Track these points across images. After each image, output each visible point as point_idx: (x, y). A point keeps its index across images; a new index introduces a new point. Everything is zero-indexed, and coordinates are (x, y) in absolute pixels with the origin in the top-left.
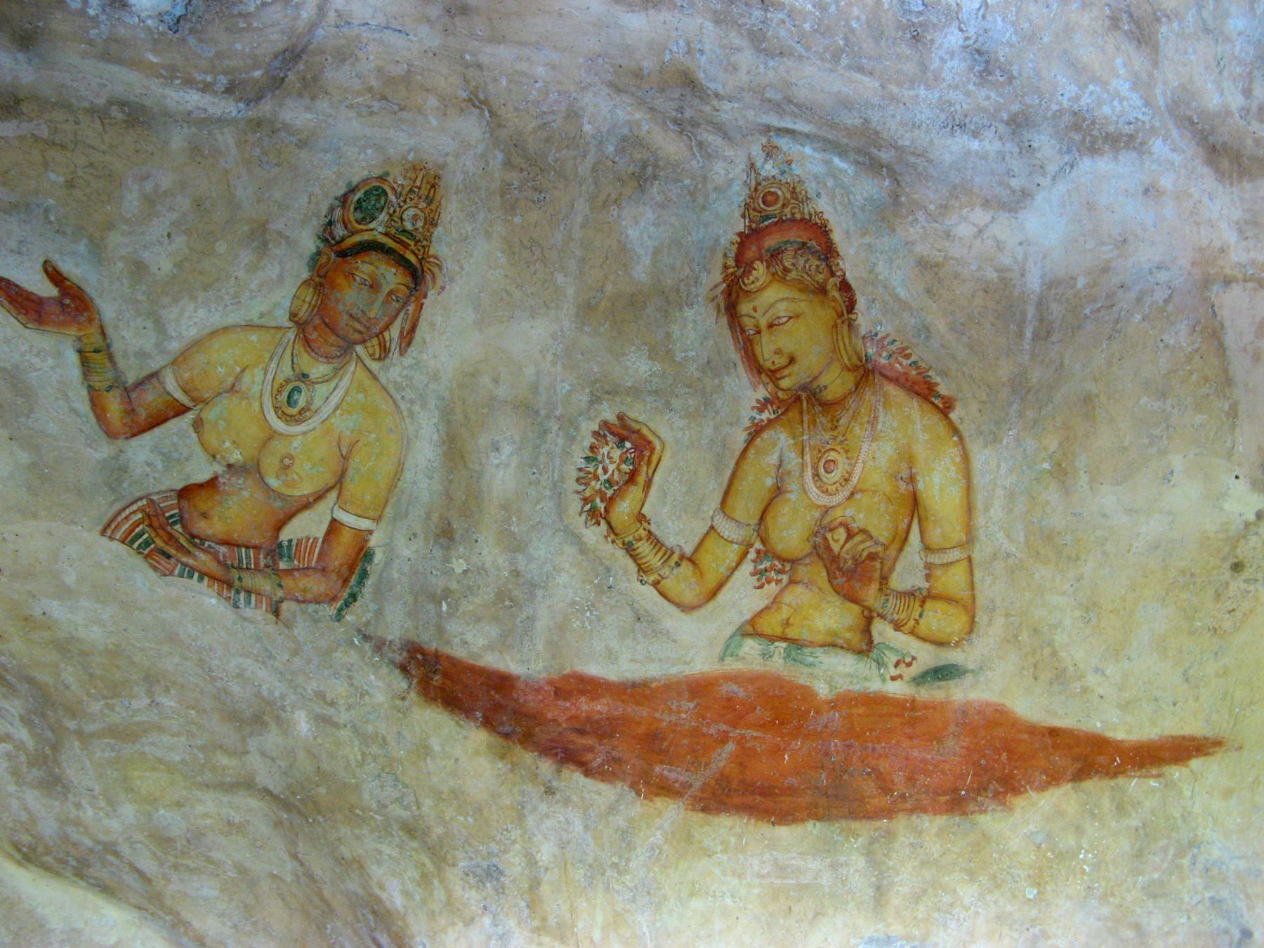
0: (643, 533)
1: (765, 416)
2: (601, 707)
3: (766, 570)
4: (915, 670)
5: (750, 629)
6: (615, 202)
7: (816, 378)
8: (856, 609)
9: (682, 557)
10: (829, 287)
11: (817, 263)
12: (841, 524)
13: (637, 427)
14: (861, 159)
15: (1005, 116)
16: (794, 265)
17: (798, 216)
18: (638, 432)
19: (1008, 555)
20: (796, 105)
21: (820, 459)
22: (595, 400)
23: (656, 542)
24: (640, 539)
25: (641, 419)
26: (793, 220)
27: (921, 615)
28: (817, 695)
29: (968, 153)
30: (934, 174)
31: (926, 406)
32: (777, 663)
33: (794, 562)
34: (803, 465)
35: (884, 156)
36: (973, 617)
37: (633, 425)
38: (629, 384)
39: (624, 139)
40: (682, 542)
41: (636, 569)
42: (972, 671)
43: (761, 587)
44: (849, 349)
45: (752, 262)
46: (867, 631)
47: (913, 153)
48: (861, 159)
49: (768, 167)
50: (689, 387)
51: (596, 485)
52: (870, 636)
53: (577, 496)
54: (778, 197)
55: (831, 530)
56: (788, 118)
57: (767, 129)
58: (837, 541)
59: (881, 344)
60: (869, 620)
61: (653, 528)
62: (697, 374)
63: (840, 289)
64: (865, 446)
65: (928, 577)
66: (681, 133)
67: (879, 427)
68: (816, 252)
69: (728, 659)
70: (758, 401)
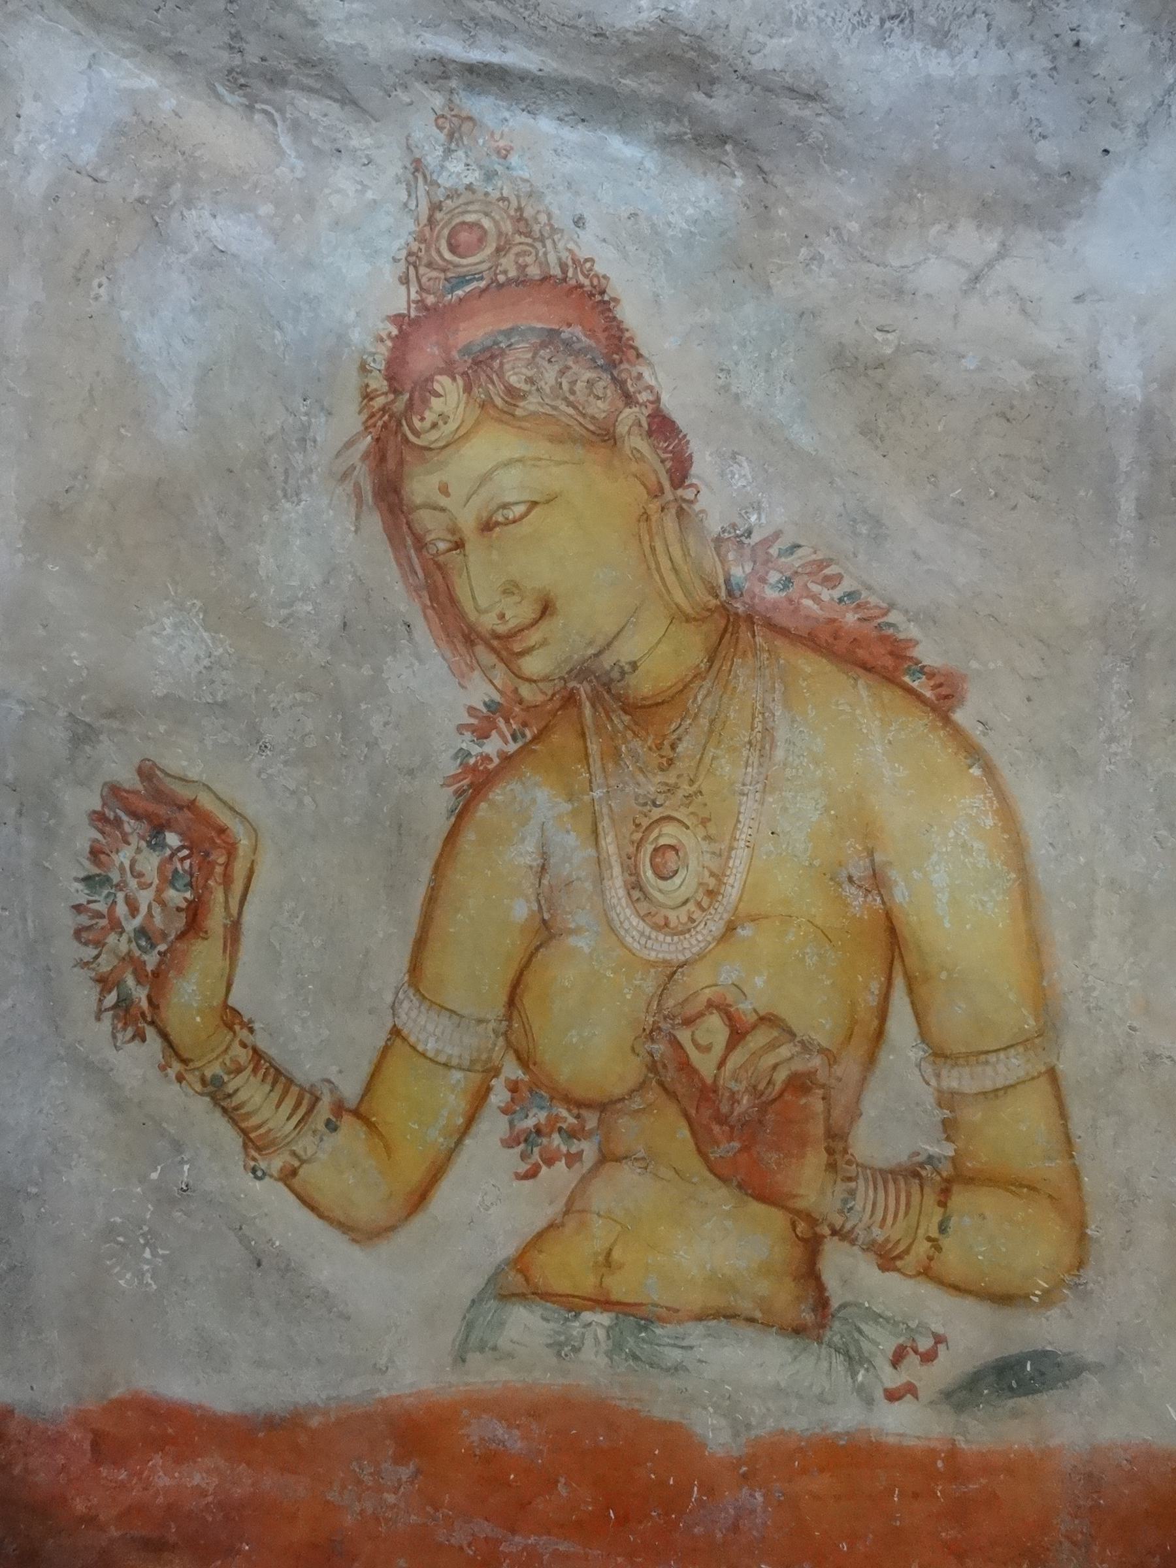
0: (243, 1055)
1: (493, 746)
2: (199, 1478)
3: (538, 1131)
5: (514, 1280)
7: (609, 645)
8: (777, 1219)
9: (339, 1108)
10: (622, 429)
11: (589, 375)
12: (711, 1005)
13: (185, 793)
14: (673, 129)
16: (530, 381)
17: (534, 272)
18: (191, 805)
19: (1154, 1058)
21: (639, 845)
22: (82, 736)
23: (277, 1077)
24: (239, 1070)
25: (192, 774)
26: (522, 281)
27: (943, 1229)
29: (928, 84)
31: (888, 694)
32: (593, 1363)
33: (603, 1107)
35: (722, 106)
36: (1082, 1225)
38: (159, 691)
39: (120, 130)
40: (332, 1072)
42: (1098, 1368)
43: (532, 1174)
44: (684, 568)
45: (430, 379)
46: (809, 1274)
47: (792, 91)
48: (673, 129)
49: (455, 166)
51: (121, 944)
52: (820, 1287)
54: (485, 232)
55: (688, 1022)
56: (485, 36)
57: (439, 71)
59: (761, 555)
60: (812, 1247)
63: (650, 433)
64: (749, 806)
65: (949, 1128)
66: (250, 108)
67: (779, 754)
69: (474, 1358)
70: (471, 710)
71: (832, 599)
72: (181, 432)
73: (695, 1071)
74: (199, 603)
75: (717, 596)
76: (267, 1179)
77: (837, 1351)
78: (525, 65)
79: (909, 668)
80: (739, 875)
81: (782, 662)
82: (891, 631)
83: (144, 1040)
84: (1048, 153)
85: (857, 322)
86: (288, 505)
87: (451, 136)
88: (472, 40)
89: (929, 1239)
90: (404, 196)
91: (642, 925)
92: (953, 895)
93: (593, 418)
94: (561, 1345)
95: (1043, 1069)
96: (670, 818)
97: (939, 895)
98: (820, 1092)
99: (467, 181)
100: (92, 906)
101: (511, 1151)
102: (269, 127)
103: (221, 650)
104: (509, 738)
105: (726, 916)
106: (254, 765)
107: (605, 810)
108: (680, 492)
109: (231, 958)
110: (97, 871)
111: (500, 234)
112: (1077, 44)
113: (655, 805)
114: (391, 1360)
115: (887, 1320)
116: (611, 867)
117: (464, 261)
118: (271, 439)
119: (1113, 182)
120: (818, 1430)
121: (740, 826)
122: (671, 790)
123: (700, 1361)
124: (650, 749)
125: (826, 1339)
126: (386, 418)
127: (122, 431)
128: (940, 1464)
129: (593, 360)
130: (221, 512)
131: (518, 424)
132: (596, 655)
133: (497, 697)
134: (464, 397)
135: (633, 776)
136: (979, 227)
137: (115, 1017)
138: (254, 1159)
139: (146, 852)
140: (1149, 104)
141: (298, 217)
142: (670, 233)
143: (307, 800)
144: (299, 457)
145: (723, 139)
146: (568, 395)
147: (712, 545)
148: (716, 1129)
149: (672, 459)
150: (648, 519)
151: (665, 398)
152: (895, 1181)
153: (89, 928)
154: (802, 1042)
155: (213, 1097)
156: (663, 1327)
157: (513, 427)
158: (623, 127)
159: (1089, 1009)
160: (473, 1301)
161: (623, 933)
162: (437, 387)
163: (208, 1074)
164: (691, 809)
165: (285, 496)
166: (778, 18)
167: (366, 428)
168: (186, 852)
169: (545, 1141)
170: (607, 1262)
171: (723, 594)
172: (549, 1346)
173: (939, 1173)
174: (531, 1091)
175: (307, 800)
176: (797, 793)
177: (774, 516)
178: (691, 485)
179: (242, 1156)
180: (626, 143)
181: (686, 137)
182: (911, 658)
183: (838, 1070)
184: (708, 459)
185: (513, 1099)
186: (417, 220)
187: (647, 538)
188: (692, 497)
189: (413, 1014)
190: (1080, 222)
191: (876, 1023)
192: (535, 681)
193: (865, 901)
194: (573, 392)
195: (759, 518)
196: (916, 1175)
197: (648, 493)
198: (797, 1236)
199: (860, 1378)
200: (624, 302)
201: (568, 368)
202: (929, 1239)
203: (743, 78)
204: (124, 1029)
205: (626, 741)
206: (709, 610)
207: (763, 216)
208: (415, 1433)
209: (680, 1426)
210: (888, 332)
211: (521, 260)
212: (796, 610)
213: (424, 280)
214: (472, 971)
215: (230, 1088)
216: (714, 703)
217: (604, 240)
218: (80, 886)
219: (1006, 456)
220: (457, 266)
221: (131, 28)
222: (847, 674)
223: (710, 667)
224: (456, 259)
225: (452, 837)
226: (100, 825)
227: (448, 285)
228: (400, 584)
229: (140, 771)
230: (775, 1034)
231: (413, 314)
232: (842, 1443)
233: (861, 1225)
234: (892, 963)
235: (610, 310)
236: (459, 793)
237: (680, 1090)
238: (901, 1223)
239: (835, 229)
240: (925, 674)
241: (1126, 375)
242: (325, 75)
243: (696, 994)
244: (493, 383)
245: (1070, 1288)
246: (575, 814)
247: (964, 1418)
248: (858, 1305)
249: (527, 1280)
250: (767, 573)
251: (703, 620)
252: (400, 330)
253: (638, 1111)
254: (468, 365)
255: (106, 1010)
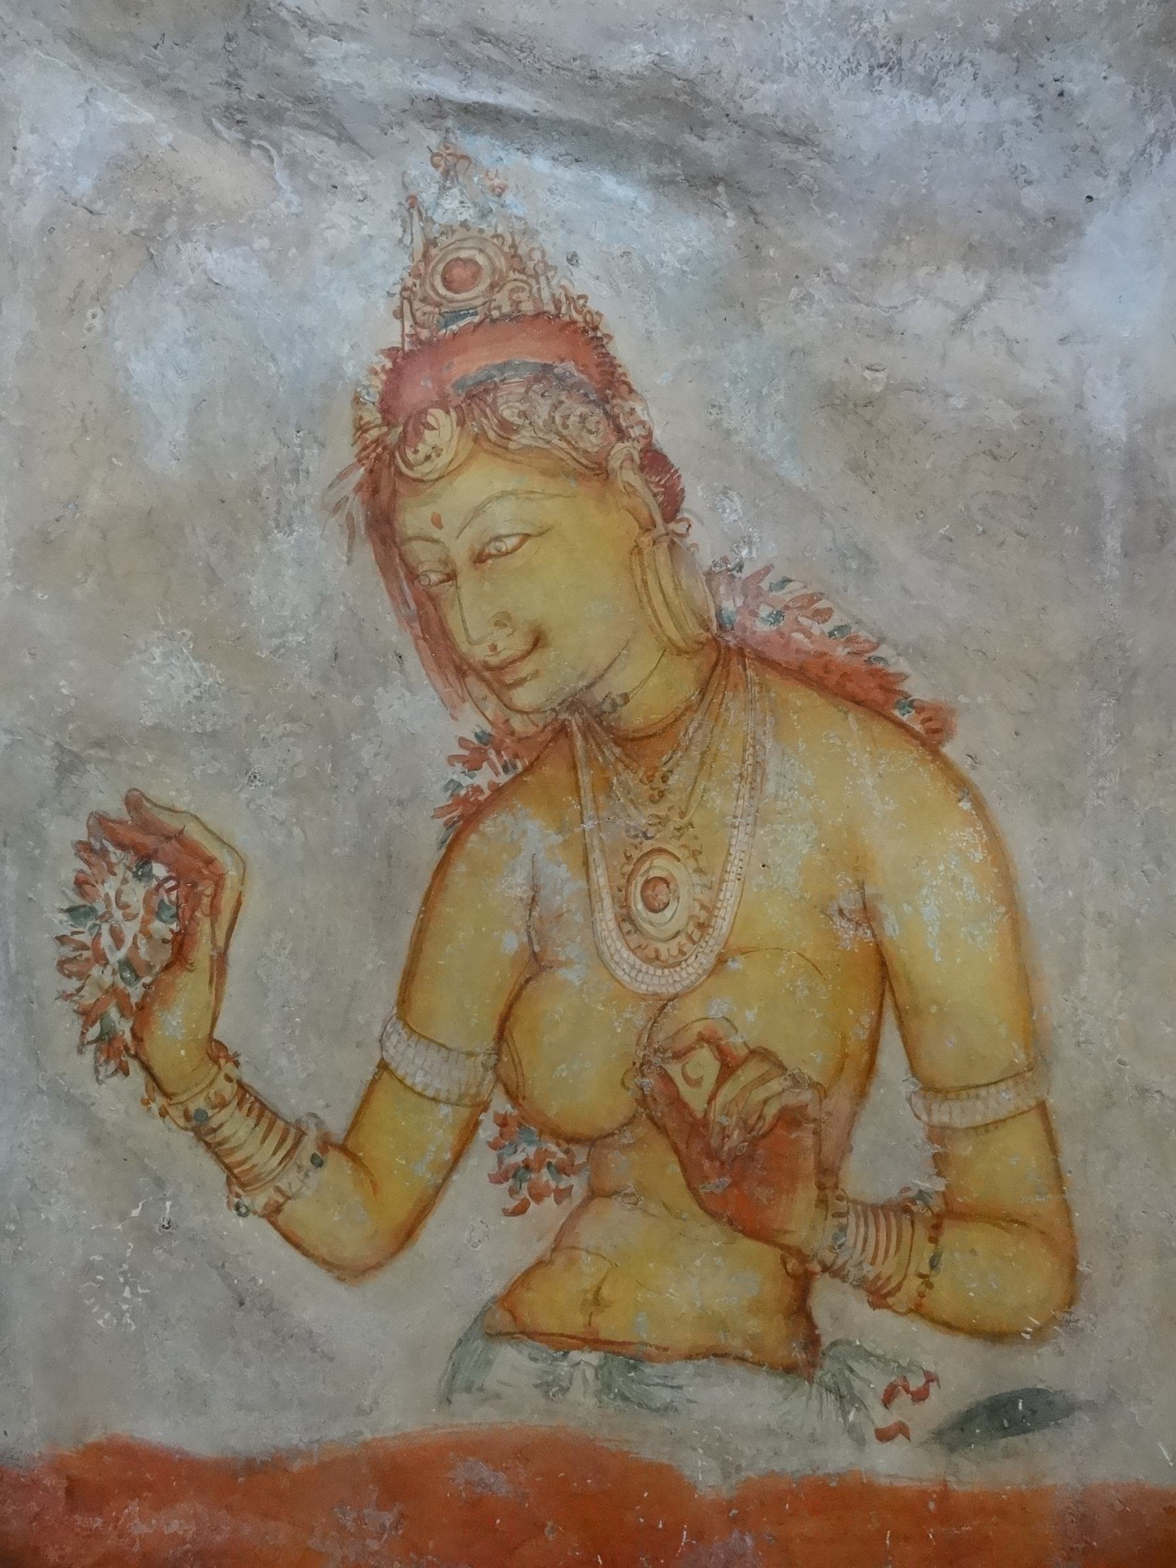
0: (228, 1090)
2: (177, 1524)
3: (527, 1167)
4: (939, 1407)
5: (501, 1319)
6: (96, 298)
7: (601, 677)
8: (768, 1255)
9: (325, 1143)
10: (614, 464)
11: (581, 409)
12: (702, 1039)
13: (173, 823)
14: (666, 170)
15: (994, 31)
16: (524, 415)
17: (528, 307)
18: (179, 836)
19: (1143, 1092)
20: (495, 40)
21: (630, 878)
22: (69, 765)
23: (262, 1111)
24: (224, 1105)
25: (180, 806)
26: (517, 317)
27: (933, 1264)
28: (693, 1488)
29: (915, 130)
30: (839, 185)
31: (879, 728)
33: (594, 1141)
34: (590, 895)
35: (715, 149)
36: (1073, 1262)
37: (165, 817)
41: (224, 1177)
43: (520, 1210)
44: (676, 602)
45: (425, 412)
46: (799, 1310)
47: (782, 135)
48: (666, 170)
49: (450, 203)
50: (292, 718)
52: (812, 1325)
53: (66, 1005)
55: (678, 1056)
56: (480, 77)
57: (435, 111)
58: (697, 1083)
59: (752, 590)
60: (802, 1284)
61: (247, 1074)
62: (310, 687)
63: (642, 468)
64: (740, 837)
65: (941, 1163)
66: (247, 143)
67: (770, 787)
68: (578, 385)
69: (461, 1398)
70: (462, 742)
71: (823, 633)
72: (174, 462)
73: (685, 1105)
74: (189, 633)
75: (708, 630)
76: (251, 1215)
77: (828, 1390)
78: (519, 105)
79: (898, 702)
80: (729, 909)
81: (773, 695)
82: (881, 665)
83: (127, 1073)
84: (1033, 198)
85: (847, 361)
86: (279, 536)
87: (446, 173)
88: (467, 81)
89: (921, 1276)
90: (399, 233)
91: (632, 957)
92: (943, 928)
93: (586, 451)
94: (548, 1384)
95: (1033, 1103)
96: (661, 851)
97: (930, 929)
98: (812, 1125)
99: (461, 218)
100: (76, 937)
101: (500, 1186)
102: (266, 163)
103: (211, 680)
104: (501, 770)
105: (717, 949)
106: (243, 796)
107: (596, 842)
108: (672, 526)
109: (217, 990)
110: (79, 901)
111: (494, 270)
112: (1061, 94)
113: (647, 838)
114: (376, 1402)
115: (878, 1358)
116: (602, 900)
117: (458, 297)
118: (264, 470)
119: (1096, 228)
120: (810, 1472)
121: (731, 858)
122: (662, 822)
123: (689, 1401)
124: (641, 781)
125: (816, 1379)
126: (379, 450)
127: (114, 460)
128: (932, 1506)
129: (586, 395)
130: (213, 542)
131: (510, 456)
132: (589, 687)
133: (488, 729)
134: (457, 430)
135: (623, 806)
136: (966, 269)
137: (98, 1050)
138: (238, 1196)
139: (133, 883)
140: (1131, 153)
141: (293, 251)
142: (663, 271)
143: (296, 830)
144: (292, 487)
145: (715, 181)
146: (560, 428)
147: (704, 578)
148: (707, 1165)
149: (664, 493)
150: (640, 553)
151: (657, 434)
152: (887, 1218)
153: (71, 960)
154: (793, 1076)
155: (196, 1131)
156: (653, 1367)
157: (505, 459)
158: (615, 169)
159: (1078, 1044)
160: (460, 1341)
161: (613, 966)
162: (430, 420)
163: (192, 1108)
164: (682, 841)
165: (277, 527)
166: (770, 65)
167: (359, 461)
168: (172, 883)
169: (533, 1176)
170: (597, 1301)
171: (714, 626)
172: (536, 1386)
173: (929, 1208)
174: (520, 1125)
175: (296, 830)
176: (788, 826)
177: (764, 550)
178: (682, 520)
179: (225, 1191)
180: (619, 183)
181: (678, 179)
182: (901, 693)
183: (829, 1104)
184: (700, 494)
185: (501, 1135)
186: (412, 256)
187: (638, 571)
188: (683, 531)
189: (401, 1047)
190: (1062, 267)
191: (866, 1057)
192: (527, 713)
193: (856, 936)
194: (565, 426)
195: (750, 552)
196: (907, 1210)
197: (640, 528)
198: (787, 1273)
199: (851, 1417)
200: (617, 338)
201: (561, 402)
202: (921, 1276)
203: (736, 122)
204: (107, 1061)
205: (618, 774)
206: (698, 643)
207: (753, 254)
208: (397, 1476)
209: (670, 1468)
210: (877, 370)
211: (515, 297)
212: (786, 645)
213: (418, 314)
214: (461, 1006)
215: (214, 1123)
216: (706, 736)
217: (597, 278)
218: (64, 917)
219: (994, 493)
220: (451, 301)
221: (129, 64)
222: (835, 707)
223: (702, 700)
224: (450, 294)
225: (443, 865)
226: (85, 856)
227: (442, 320)
228: (392, 614)
229: (127, 801)
230: (766, 1067)
231: (407, 348)
232: (834, 1484)
233: (852, 1262)
234: (882, 996)
235: (603, 346)
236: (449, 825)
237: (671, 1124)
238: (893, 1260)
239: (826, 269)
240: (914, 708)
241: (1110, 415)
242: (323, 113)
243: (686, 1027)
244: (486, 417)
245: (1061, 1326)
246: (566, 845)
247: (956, 1458)
248: (849, 1343)
249: (515, 1318)
250: (758, 607)
251: (695, 653)
252: (394, 363)
253: (629, 1146)
254: (462, 398)
255: (89, 1043)
